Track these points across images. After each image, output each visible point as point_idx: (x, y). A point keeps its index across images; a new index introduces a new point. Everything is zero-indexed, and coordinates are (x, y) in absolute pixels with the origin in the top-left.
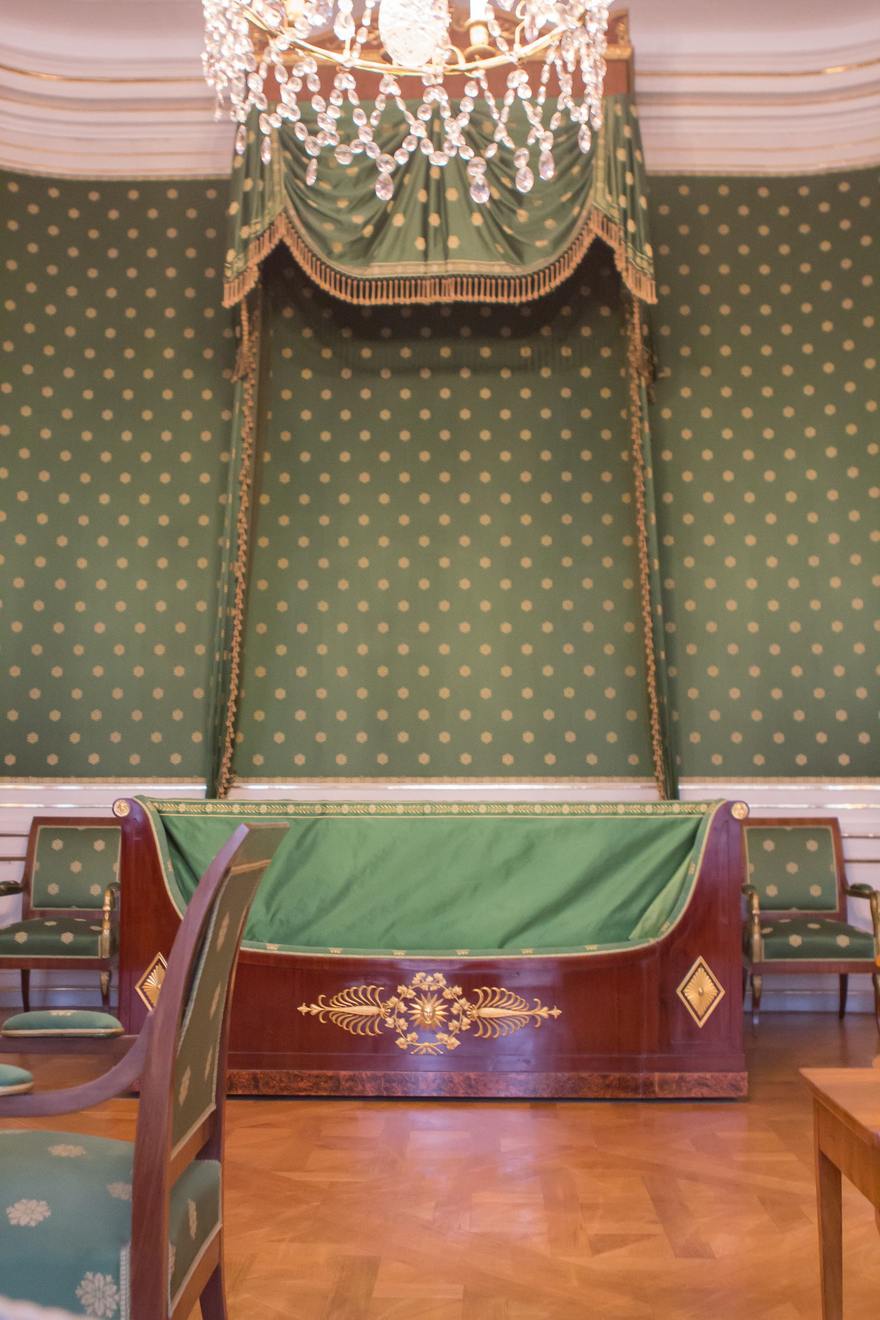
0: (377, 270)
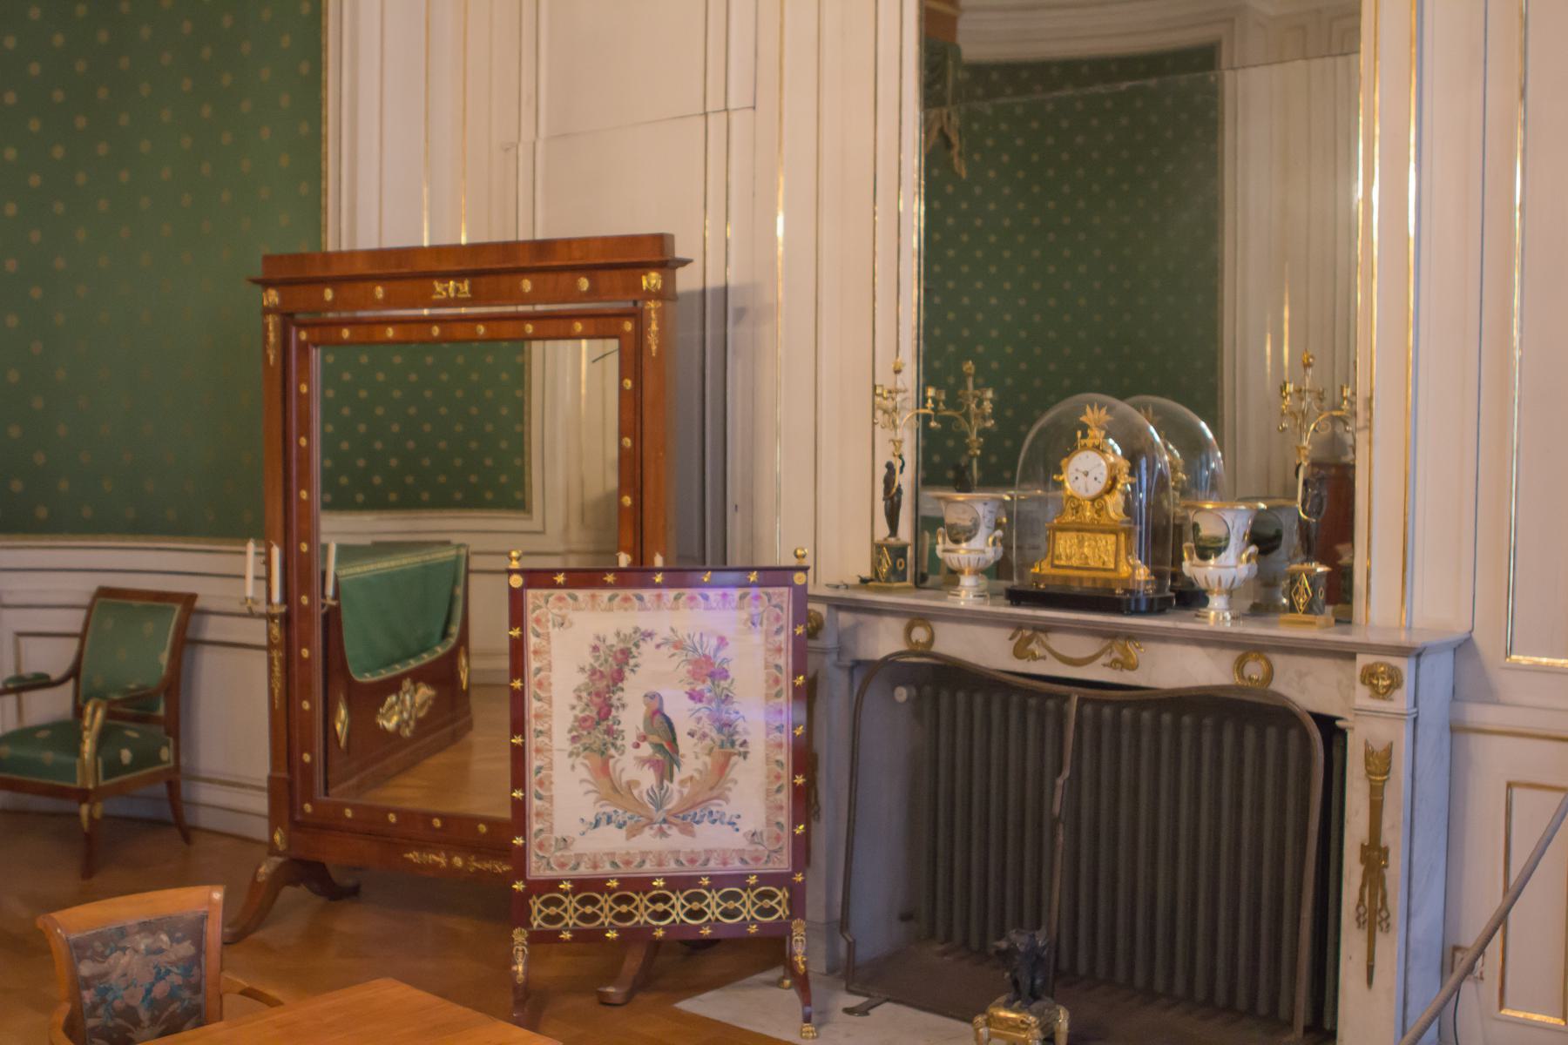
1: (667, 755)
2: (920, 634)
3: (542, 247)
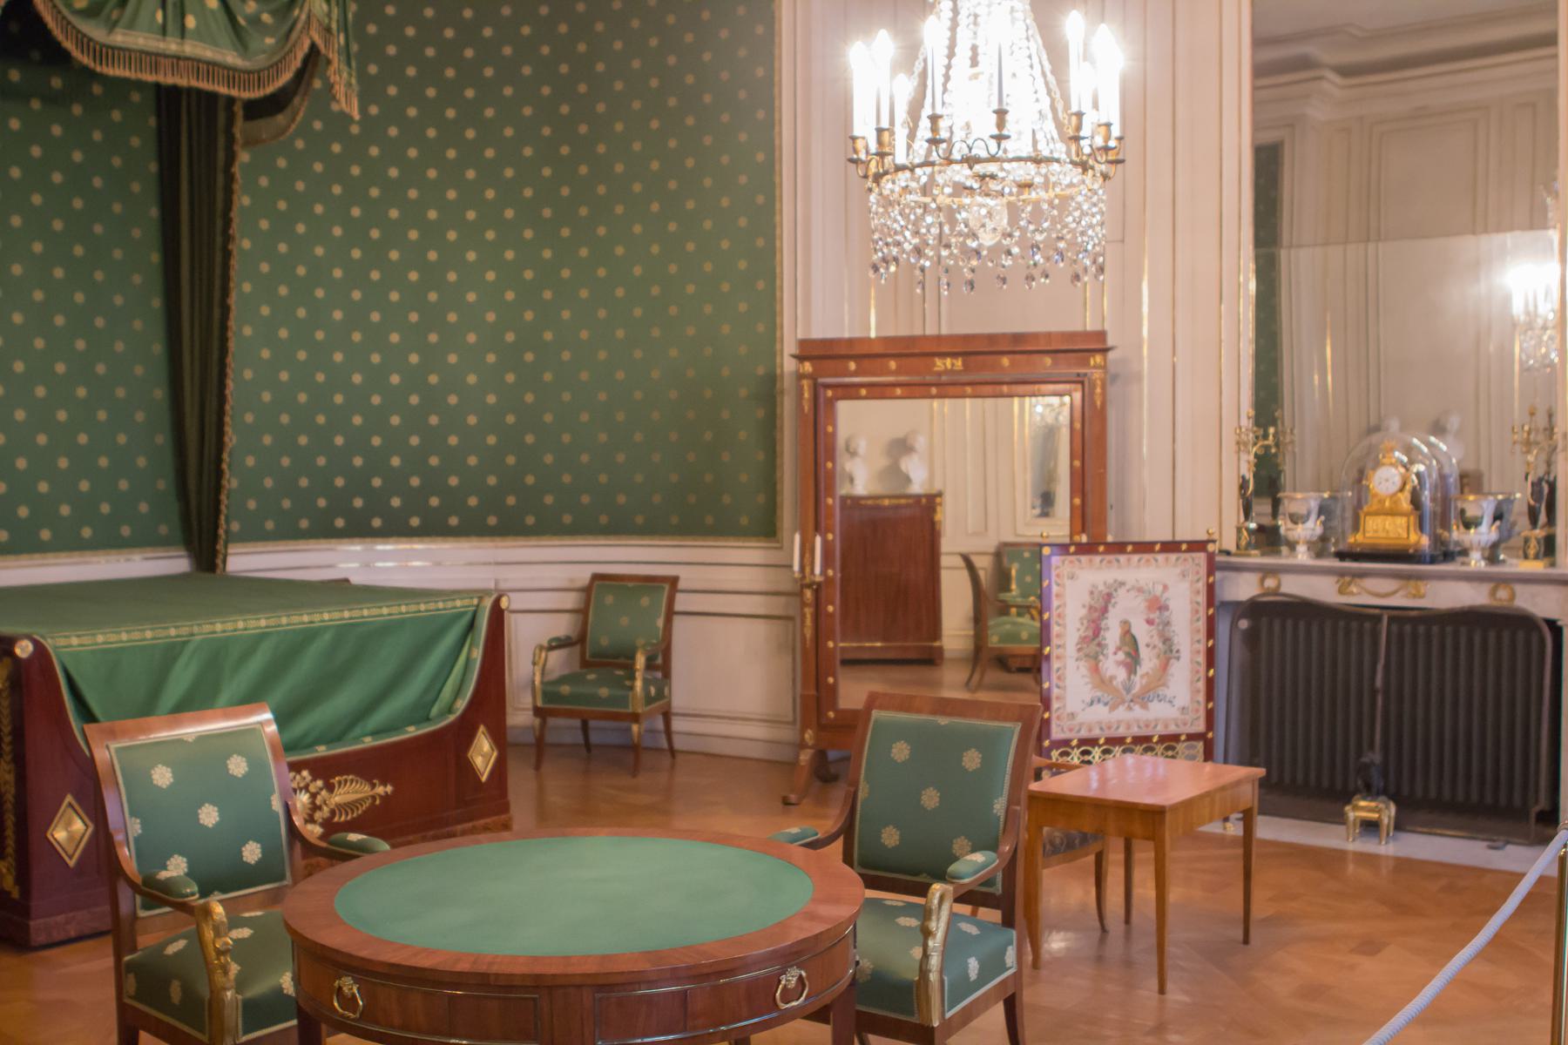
0: (119, 38)
1: (1133, 660)
2: (1270, 583)
3: (1017, 338)
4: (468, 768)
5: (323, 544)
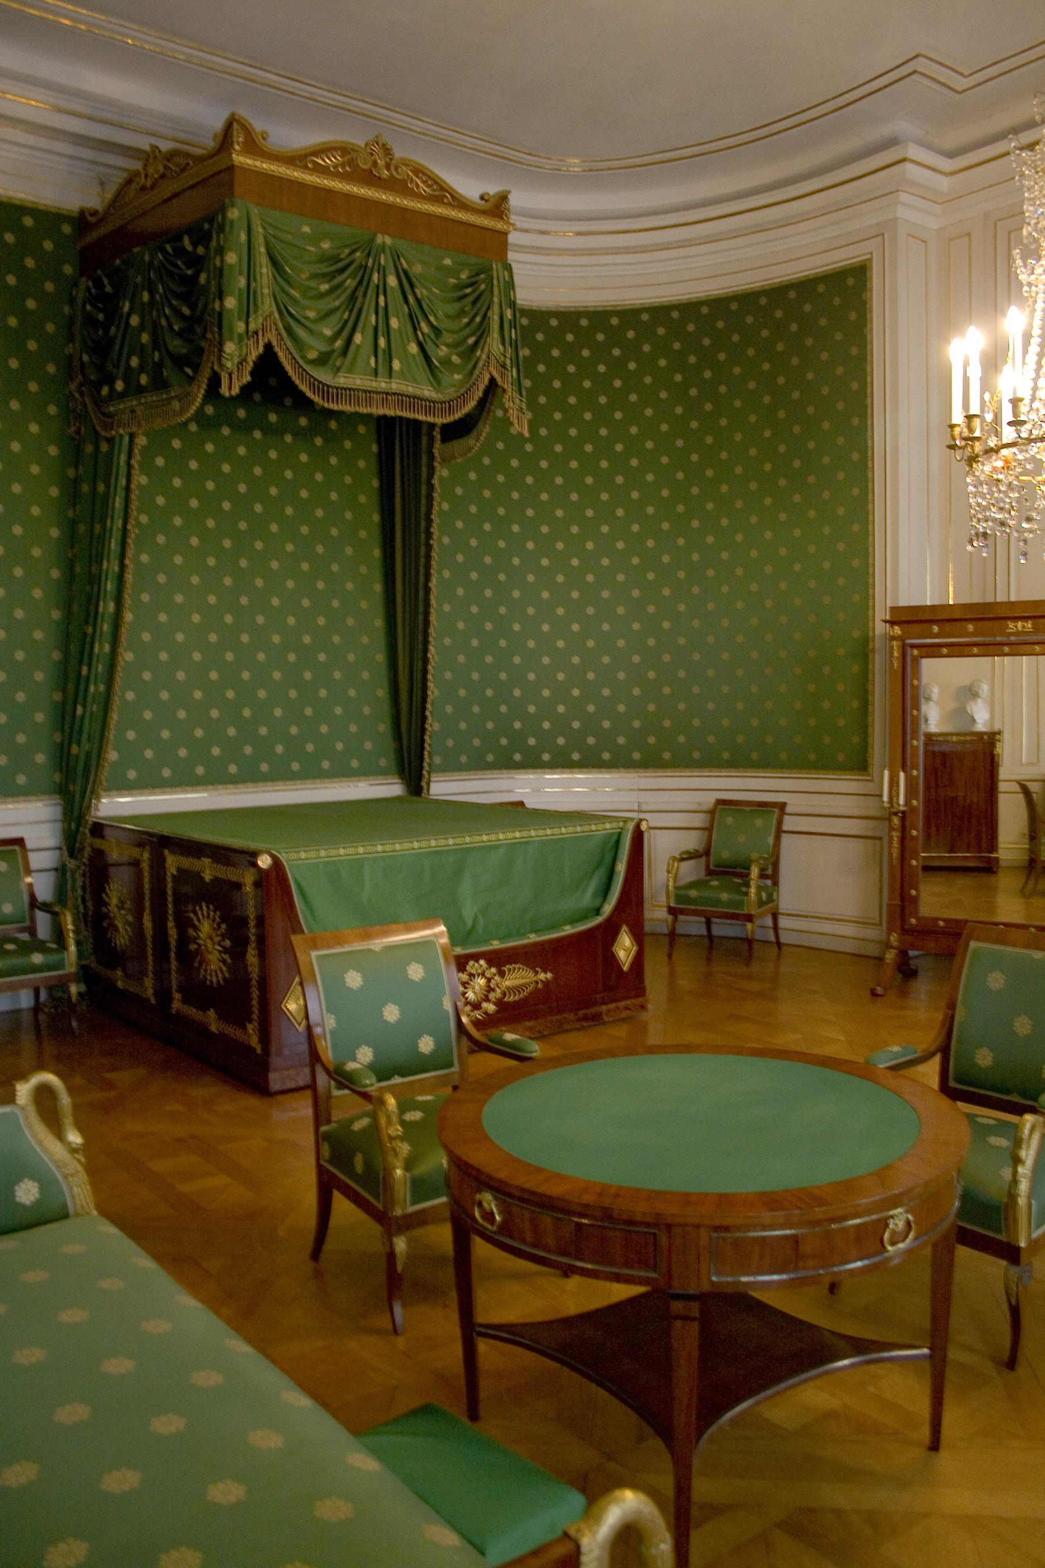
0: (341, 381)
4: (611, 959)
5: (505, 774)
